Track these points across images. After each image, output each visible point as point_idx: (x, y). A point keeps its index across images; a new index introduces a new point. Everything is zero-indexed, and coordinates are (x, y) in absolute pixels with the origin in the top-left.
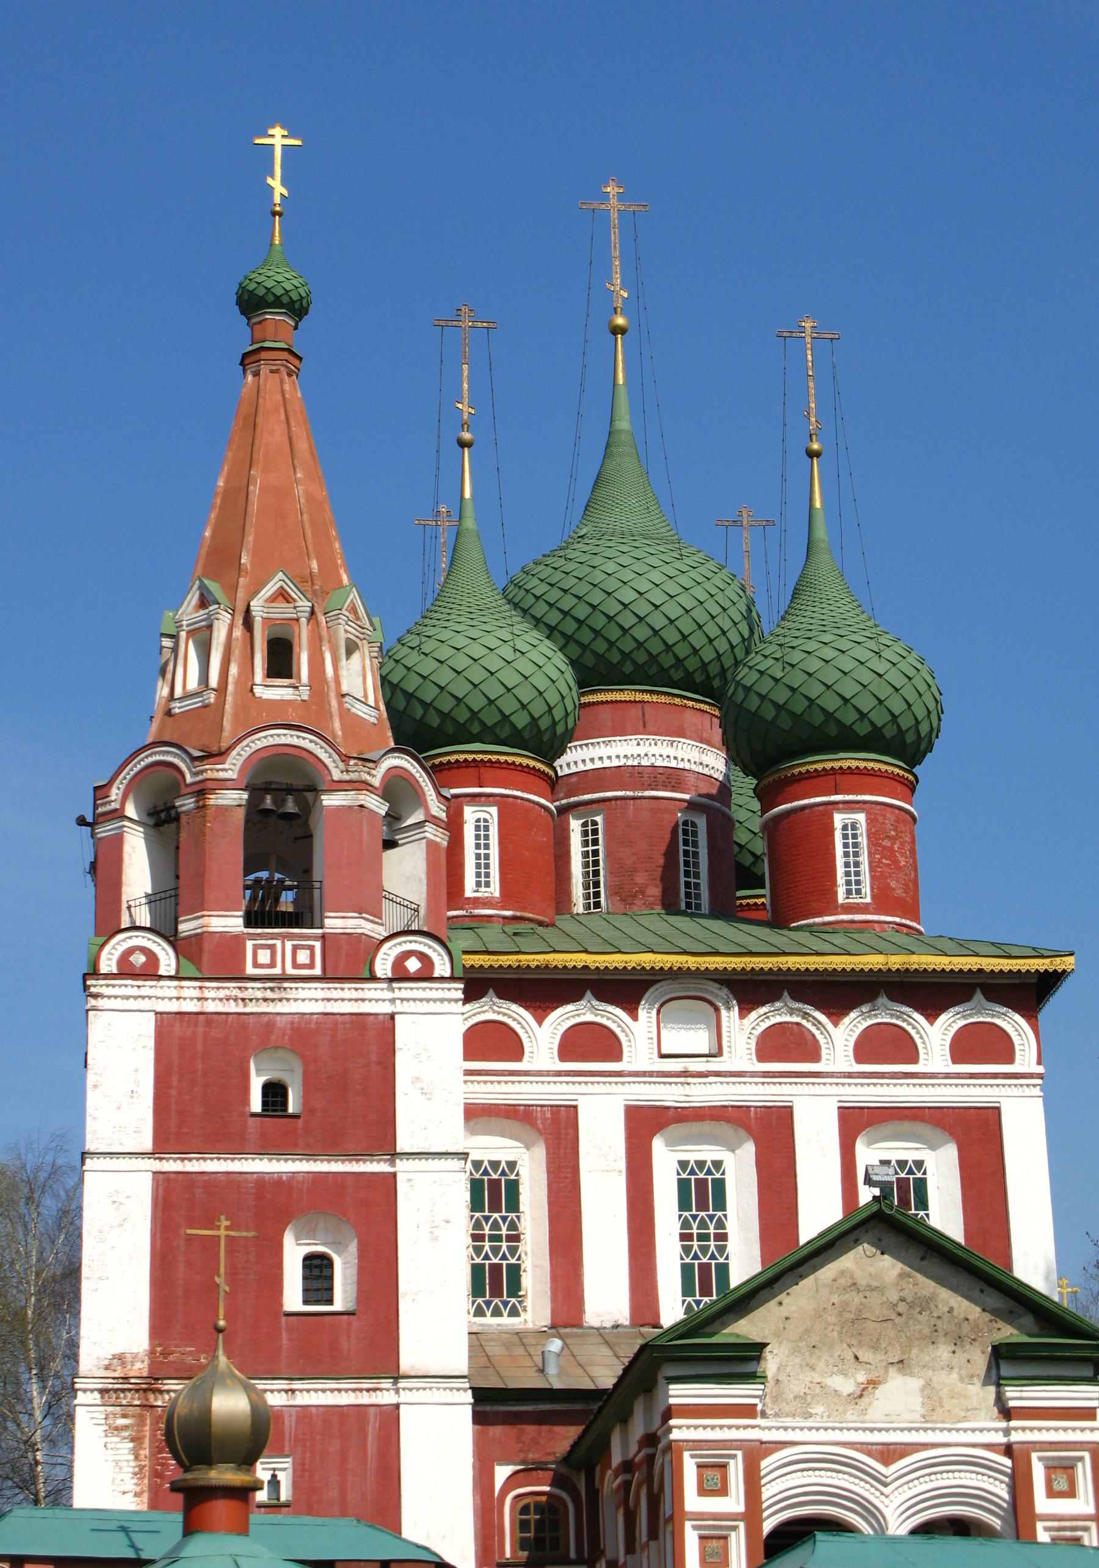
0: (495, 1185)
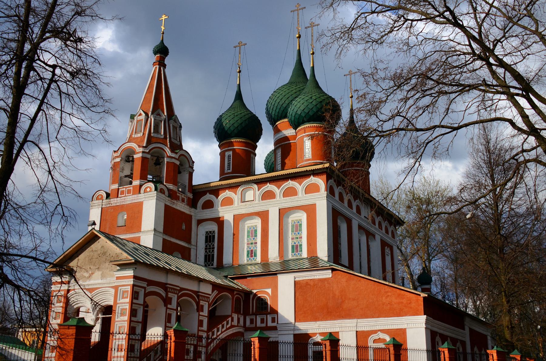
0: (210, 236)
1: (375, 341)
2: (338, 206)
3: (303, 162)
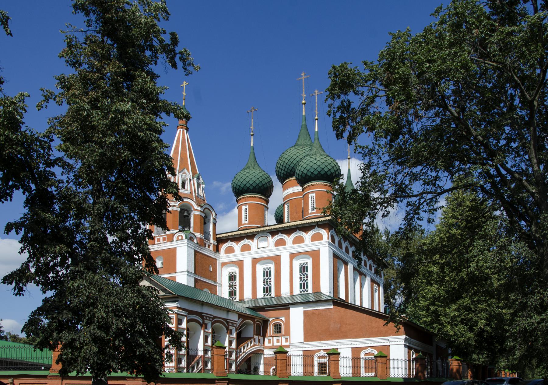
0: (232, 276)
1: (366, 354)
2: (338, 252)
3: (308, 214)
